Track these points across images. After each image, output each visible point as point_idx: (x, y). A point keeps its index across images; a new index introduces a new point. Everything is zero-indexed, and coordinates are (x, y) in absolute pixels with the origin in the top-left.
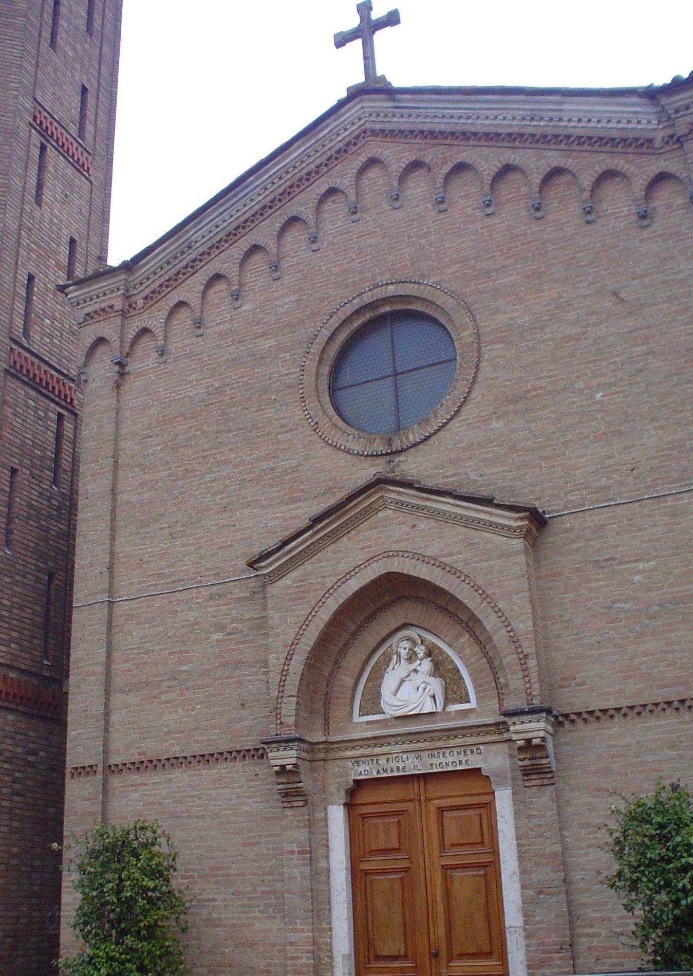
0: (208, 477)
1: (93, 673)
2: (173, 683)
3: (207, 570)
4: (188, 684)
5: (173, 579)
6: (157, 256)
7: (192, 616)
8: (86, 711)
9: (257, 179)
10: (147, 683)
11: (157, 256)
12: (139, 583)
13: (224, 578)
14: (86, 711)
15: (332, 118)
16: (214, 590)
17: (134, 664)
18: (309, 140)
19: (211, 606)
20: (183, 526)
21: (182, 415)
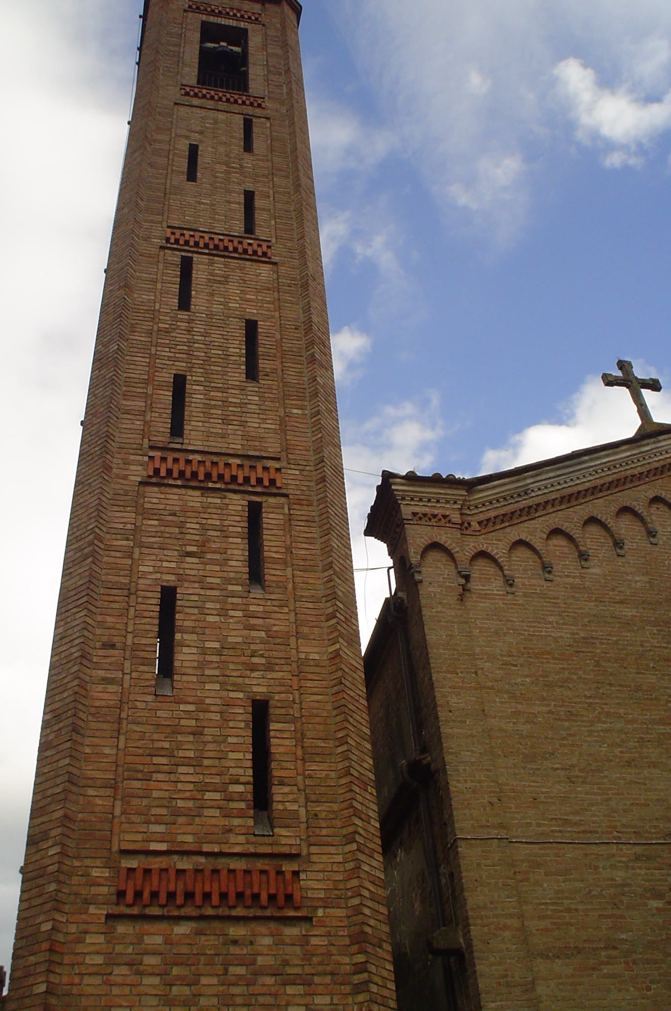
0: (599, 726)
1: (506, 927)
2: (615, 953)
3: (623, 825)
4: (634, 956)
5: (582, 828)
6: (494, 487)
7: (619, 875)
8: (506, 976)
9: (591, 460)
10: (579, 951)
11: (494, 487)
12: (538, 825)
13: (647, 838)
14: (506, 976)
15: (652, 440)
16: (638, 849)
17: (552, 923)
18: (633, 449)
19: (640, 868)
20: (581, 771)
21: (549, 653)
